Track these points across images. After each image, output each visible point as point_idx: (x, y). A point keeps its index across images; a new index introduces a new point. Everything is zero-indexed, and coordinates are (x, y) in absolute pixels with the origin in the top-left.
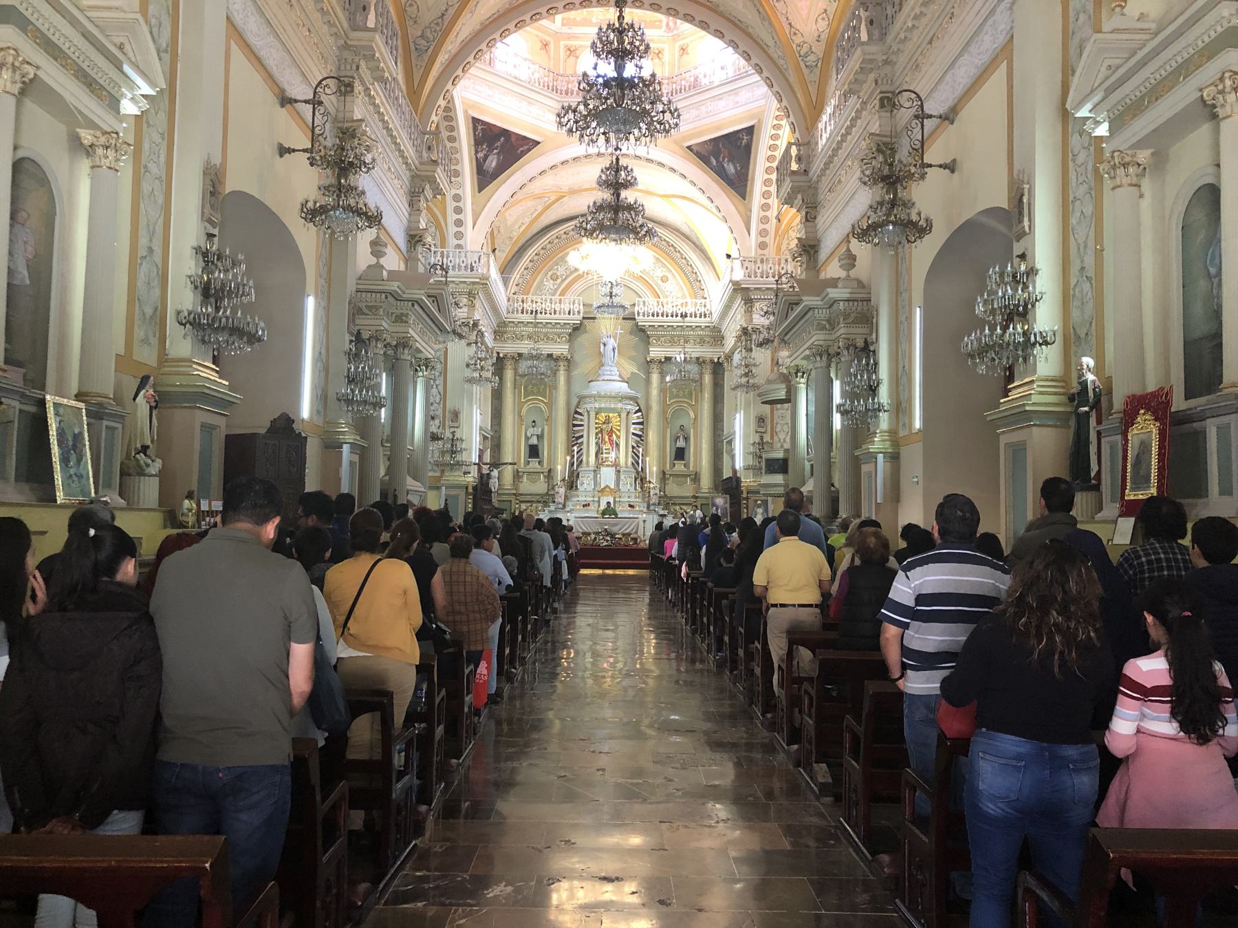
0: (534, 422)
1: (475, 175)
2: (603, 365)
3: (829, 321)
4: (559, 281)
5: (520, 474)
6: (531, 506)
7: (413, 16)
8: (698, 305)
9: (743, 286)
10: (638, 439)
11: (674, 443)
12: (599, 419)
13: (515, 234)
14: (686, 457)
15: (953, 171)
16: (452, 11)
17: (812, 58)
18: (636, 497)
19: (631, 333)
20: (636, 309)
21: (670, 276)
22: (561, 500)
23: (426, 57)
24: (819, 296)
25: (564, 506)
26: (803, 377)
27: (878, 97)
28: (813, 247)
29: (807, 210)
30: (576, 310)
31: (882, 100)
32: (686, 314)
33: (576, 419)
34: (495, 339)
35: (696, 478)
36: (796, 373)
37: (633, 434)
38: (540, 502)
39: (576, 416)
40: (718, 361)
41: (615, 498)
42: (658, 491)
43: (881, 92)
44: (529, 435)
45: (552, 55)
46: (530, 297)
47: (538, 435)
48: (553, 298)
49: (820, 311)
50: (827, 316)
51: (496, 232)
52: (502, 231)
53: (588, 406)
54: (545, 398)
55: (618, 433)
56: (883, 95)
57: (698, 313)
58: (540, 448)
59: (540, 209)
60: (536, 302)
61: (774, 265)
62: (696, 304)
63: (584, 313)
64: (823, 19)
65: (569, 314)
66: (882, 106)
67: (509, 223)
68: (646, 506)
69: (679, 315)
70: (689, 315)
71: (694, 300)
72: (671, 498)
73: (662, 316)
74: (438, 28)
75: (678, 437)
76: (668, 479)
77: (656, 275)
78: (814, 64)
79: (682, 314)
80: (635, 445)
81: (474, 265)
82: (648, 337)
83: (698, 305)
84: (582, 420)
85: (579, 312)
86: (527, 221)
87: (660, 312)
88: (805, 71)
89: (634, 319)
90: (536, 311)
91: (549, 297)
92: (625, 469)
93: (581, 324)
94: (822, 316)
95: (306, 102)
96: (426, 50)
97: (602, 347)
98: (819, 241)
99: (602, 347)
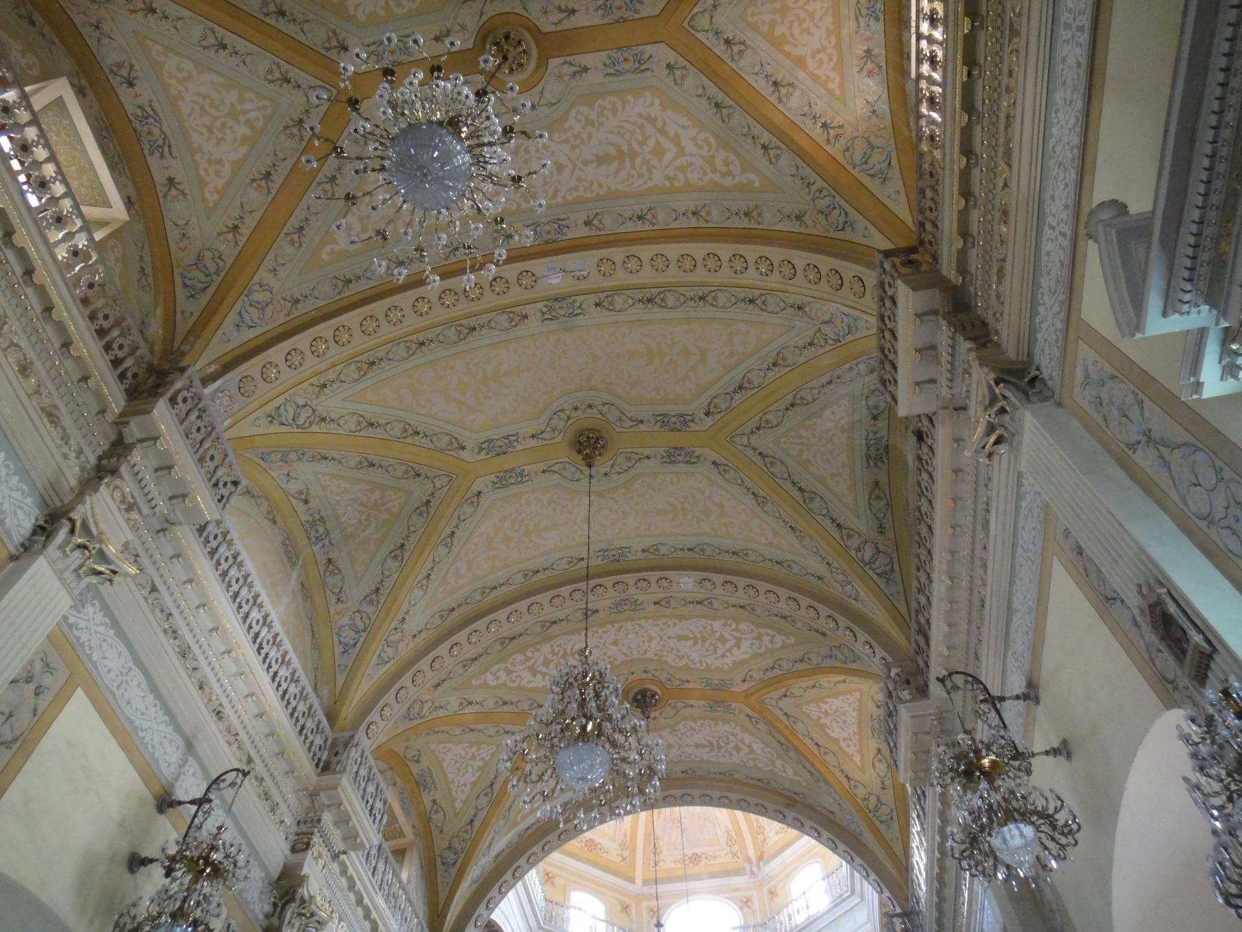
7: (440, 824)
15: (1069, 756)
16: (481, 816)
17: (884, 811)
23: (454, 871)
45: (634, 918)
64: (880, 761)
78: (889, 817)
88: (882, 828)
95: (192, 802)
96: (454, 864)
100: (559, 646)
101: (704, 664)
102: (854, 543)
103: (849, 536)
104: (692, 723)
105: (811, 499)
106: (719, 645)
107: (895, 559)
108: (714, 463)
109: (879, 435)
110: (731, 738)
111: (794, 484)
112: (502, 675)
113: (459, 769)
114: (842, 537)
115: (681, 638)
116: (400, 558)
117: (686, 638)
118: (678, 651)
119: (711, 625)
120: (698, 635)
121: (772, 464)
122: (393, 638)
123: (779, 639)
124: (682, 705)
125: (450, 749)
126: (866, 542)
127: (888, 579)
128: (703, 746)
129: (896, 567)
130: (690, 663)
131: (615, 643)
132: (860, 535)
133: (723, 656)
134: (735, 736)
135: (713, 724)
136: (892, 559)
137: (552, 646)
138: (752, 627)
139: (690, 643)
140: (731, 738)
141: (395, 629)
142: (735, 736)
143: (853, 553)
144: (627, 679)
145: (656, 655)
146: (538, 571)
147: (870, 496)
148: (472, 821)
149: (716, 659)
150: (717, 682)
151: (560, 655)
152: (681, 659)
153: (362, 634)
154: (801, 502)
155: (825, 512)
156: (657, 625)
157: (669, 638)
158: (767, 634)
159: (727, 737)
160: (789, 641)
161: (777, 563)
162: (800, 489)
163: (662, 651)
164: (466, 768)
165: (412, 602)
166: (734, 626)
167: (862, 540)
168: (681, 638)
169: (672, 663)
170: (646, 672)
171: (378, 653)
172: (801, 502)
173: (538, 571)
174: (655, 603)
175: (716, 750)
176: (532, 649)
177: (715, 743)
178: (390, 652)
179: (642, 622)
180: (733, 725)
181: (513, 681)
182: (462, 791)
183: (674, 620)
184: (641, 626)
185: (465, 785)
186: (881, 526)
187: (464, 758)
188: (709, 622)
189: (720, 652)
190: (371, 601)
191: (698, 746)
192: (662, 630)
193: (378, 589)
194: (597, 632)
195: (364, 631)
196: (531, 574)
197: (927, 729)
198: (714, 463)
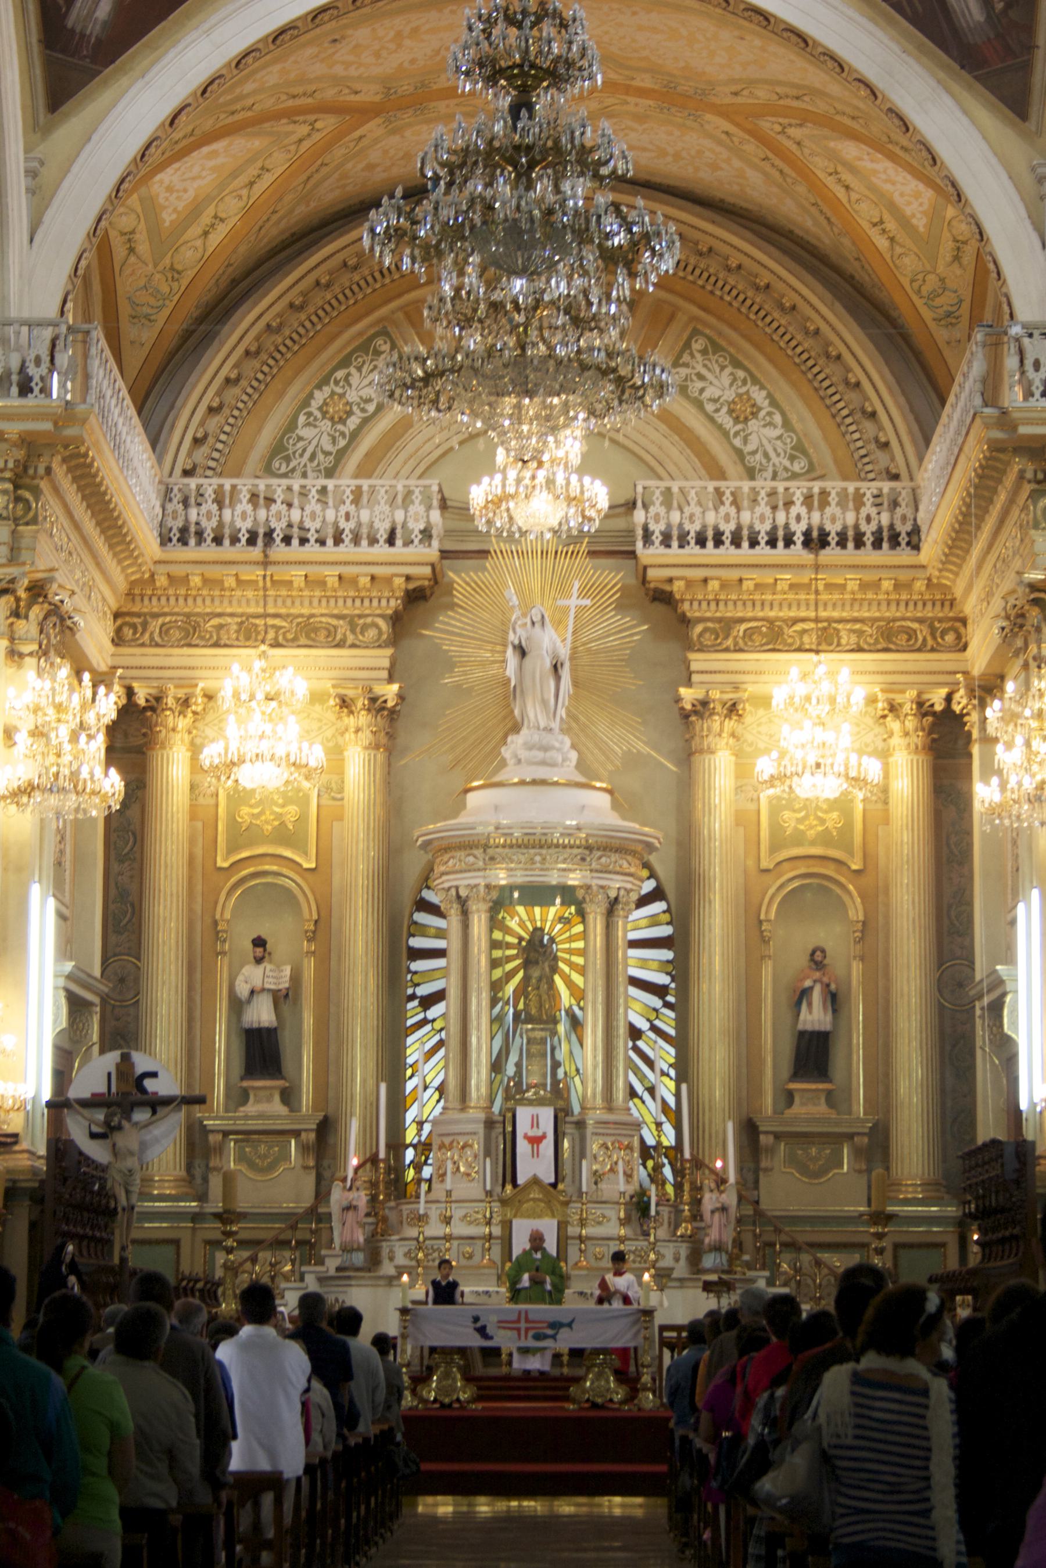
0: (259, 942)
1: (36, 48)
4: (353, 422)
5: (214, 1139)
6: (254, 1260)
8: (868, 500)
9: (1023, 430)
10: (656, 1002)
12: (508, 931)
13: (189, 257)
19: (621, 607)
20: (639, 516)
21: (759, 396)
25: (374, 1260)
33: (422, 930)
34: (118, 640)
37: (635, 982)
38: (280, 1244)
39: (421, 917)
40: (948, 709)
41: (562, 1226)
42: (730, 1198)
44: (242, 990)
46: (245, 485)
48: (330, 484)
51: (119, 250)
52: (143, 248)
53: (464, 881)
54: (306, 853)
55: (578, 979)
57: (868, 529)
58: (286, 1040)
59: (279, 162)
60: (270, 501)
62: (859, 500)
63: (448, 533)
65: (391, 541)
67: (168, 218)
68: (684, 1250)
69: (799, 538)
70: (833, 539)
71: (851, 487)
72: (777, 1223)
73: (666, 541)
75: (804, 994)
76: (771, 1151)
77: (711, 392)
79: (807, 534)
80: (643, 1025)
81: (32, 370)
82: (685, 621)
83: (868, 500)
84: (441, 934)
85: (427, 534)
86: (232, 208)
87: (728, 528)
89: (632, 554)
90: (269, 535)
91: (315, 483)
93: (435, 578)
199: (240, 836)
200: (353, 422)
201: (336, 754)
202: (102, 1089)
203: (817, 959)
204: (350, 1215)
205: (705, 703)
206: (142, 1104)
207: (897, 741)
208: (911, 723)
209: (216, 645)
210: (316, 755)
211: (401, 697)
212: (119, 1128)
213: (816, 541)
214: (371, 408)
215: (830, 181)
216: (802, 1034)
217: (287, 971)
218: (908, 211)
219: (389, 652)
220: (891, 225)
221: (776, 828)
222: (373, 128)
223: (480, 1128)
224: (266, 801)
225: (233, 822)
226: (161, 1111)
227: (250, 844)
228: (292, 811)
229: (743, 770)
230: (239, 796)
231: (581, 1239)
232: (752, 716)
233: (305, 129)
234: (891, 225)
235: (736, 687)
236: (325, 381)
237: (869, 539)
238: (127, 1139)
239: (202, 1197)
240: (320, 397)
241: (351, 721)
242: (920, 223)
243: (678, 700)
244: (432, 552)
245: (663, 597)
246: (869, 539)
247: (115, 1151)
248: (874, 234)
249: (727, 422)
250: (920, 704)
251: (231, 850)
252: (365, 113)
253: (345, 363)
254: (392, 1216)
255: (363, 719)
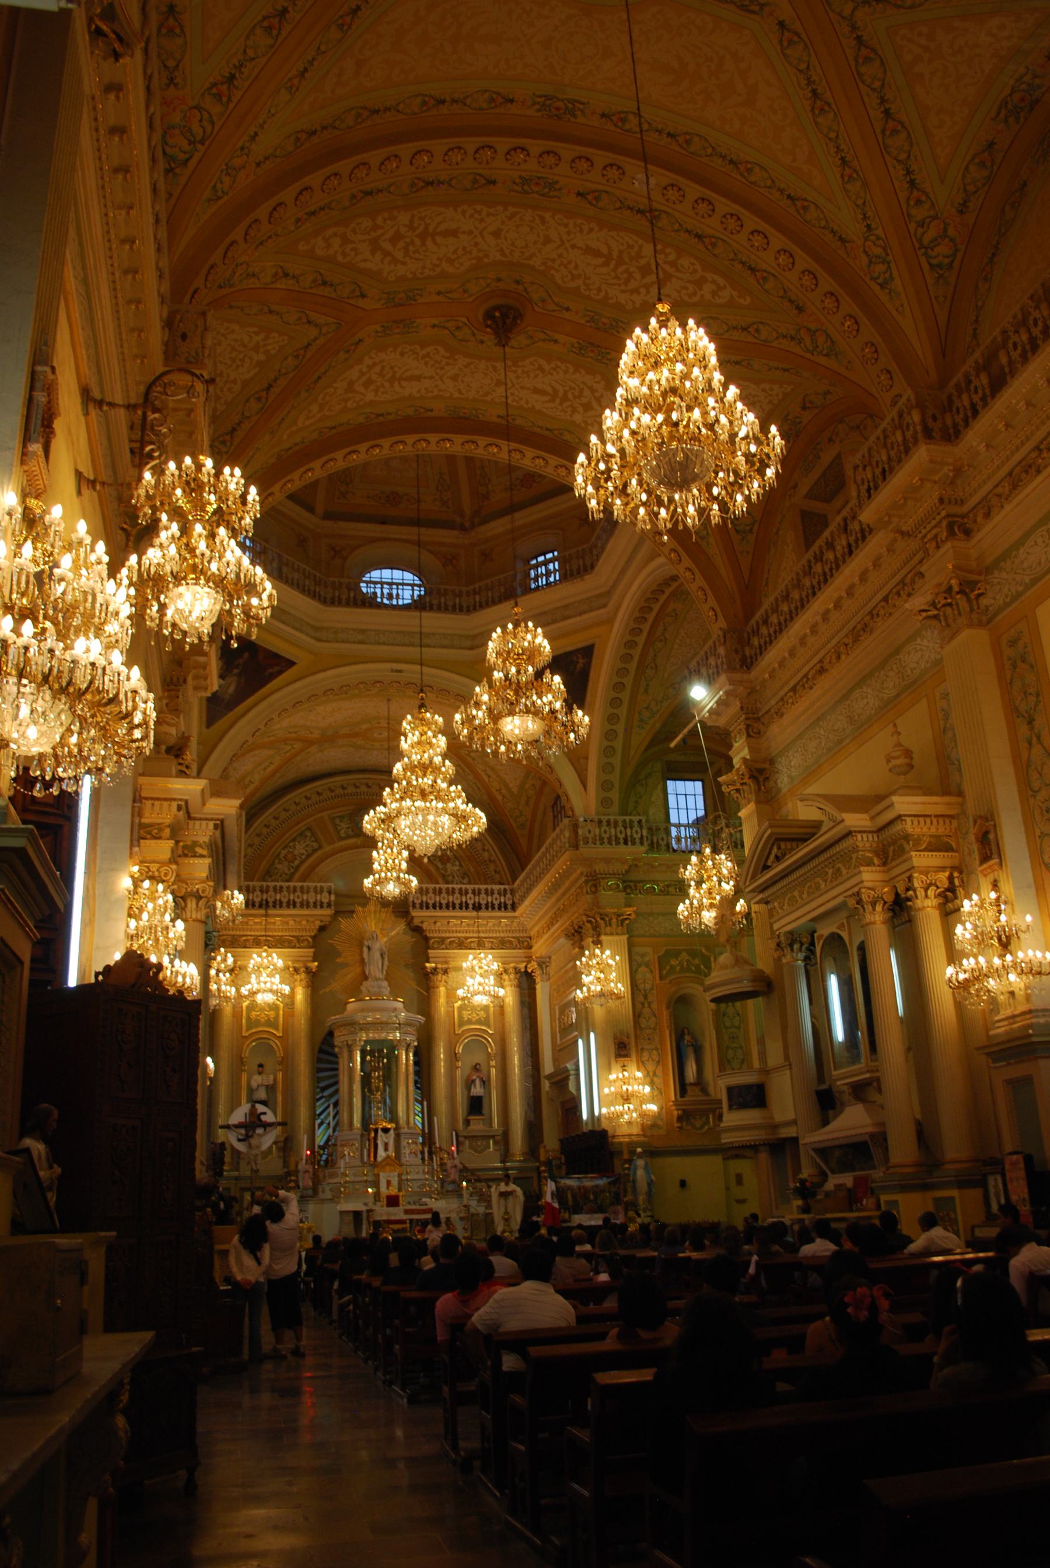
0: (261, 1066)
2: (366, 978)
3: (876, 853)
4: (297, 862)
11: (466, 1092)
14: (485, 1110)
18: (424, 1173)
22: (306, 1181)
24: (866, 812)
25: (315, 1192)
26: (800, 950)
27: (944, 523)
28: (761, 771)
29: (748, 722)
30: (326, 901)
31: (950, 527)
32: (480, 904)
35: (505, 1139)
36: (791, 945)
40: (526, 972)
41: (400, 1175)
43: (948, 516)
44: (254, 1085)
47: (267, 1087)
49: (865, 836)
50: (874, 845)
54: (277, 1029)
56: (950, 519)
61: (625, 828)
63: (336, 904)
66: (951, 534)
69: (471, 906)
70: (483, 906)
74: (225, 450)
75: (473, 1081)
78: (748, 528)
79: (474, 905)
82: (427, 939)
91: (285, 884)
92: (406, 1130)
94: (868, 845)
97: (365, 950)
98: (772, 762)
99: (365, 950)
100: (421, 218)
101: (602, 294)
102: (920, 213)
103: (918, 202)
104: (543, 362)
105: (894, 132)
106: (638, 276)
107: (960, 255)
108: (781, 24)
109: (1037, 81)
110: (587, 393)
111: (883, 100)
112: (336, 242)
113: (233, 360)
114: (908, 199)
115: (589, 251)
116: (275, 32)
117: (597, 253)
118: (576, 267)
119: (641, 247)
120: (615, 254)
121: (867, 60)
122: (237, 162)
123: (727, 294)
124: (542, 336)
125: (233, 332)
126: (936, 217)
127: (941, 276)
128: (543, 393)
129: (956, 264)
130: (583, 288)
131: (496, 234)
132: (933, 204)
133: (636, 291)
134: (592, 390)
135: (571, 370)
136: (957, 250)
137: (413, 216)
138: (698, 267)
139: (600, 261)
140: (587, 393)
141: (242, 149)
142: (592, 390)
143: (912, 226)
144: (488, 285)
145: (544, 264)
146: (442, 102)
147: (974, 157)
148: (234, 430)
149: (622, 291)
150: (605, 320)
151: (418, 232)
152: (574, 278)
153: (199, 146)
154: (878, 130)
155: (903, 156)
156: (566, 225)
157: (573, 246)
158: (714, 282)
159: (582, 390)
160: (741, 301)
161: (789, 197)
162: (887, 113)
163: (554, 260)
164: (243, 360)
165: (273, 111)
166: (672, 257)
167: (932, 213)
168: (589, 251)
169: (559, 281)
170: (517, 282)
171: (212, 184)
172: (878, 130)
173: (442, 102)
174: (579, 194)
175: (558, 401)
176: (386, 215)
177: (561, 394)
178: (227, 180)
179: (547, 215)
180: (598, 377)
181: (344, 254)
182: (230, 390)
183: (593, 225)
184: (543, 220)
185: (235, 382)
186: (964, 204)
187: (245, 346)
188: (640, 242)
189: (633, 285)
190: (219, 96)
191: (536, 391)
192: (569, 233)
193: (232, 77)
194: (479, 212)
195: (202, 142)
196: (432, 102)
197: (937, 478)
198: (781, 24)
199: (251, 1023)
200: (297, 862)
201: (292, 990)
202: (243, 1120)
203: (476, 1068)
204: (307, 1175)
205: (435, 969)
206: (259, 1126)
207: (506, 983)
208: (512, 976)
209: (245, 947)
210: (287, 989)
211: (317, 967)
212: (252, 1136)
213: (477, 907)
214: (304, 857)
215: (483, 774)
216: (473, 1098)
217: (272, 1077)
218: (511, 785)
219: (312, 950)
220: (504, 791)
221: (460, 1016)
222: (313, 749)
223: (359, 1137)
224: (262, 1009)
225: (249, 1018)
226: (268, 1129)
227: (256, 1026)
228: (272, 1014)
229: (451, 996)
230: (253, 1006)
231: (407, 1180)
232: (452, 975)
233: (289, 748)
234: (504, 791)
235: (447, 962)
236: (286, 847)
237: (496, 906)
238: (254, 1141)
239: (238, 1170)
240: (284, 852)
241: (298, 977)
242: (515, 790)
243: (425, 967)
244: (329, 912)
245: (418, 930)
246: (496, 906)
247: (250, 1146)
248: (497, 794)
249: (439, 865)
250: (515, 968)
251: (249, 1028)
252: (310, 743)
253: (294, 840)
254: (321, 1175)
255: (303, 976)
